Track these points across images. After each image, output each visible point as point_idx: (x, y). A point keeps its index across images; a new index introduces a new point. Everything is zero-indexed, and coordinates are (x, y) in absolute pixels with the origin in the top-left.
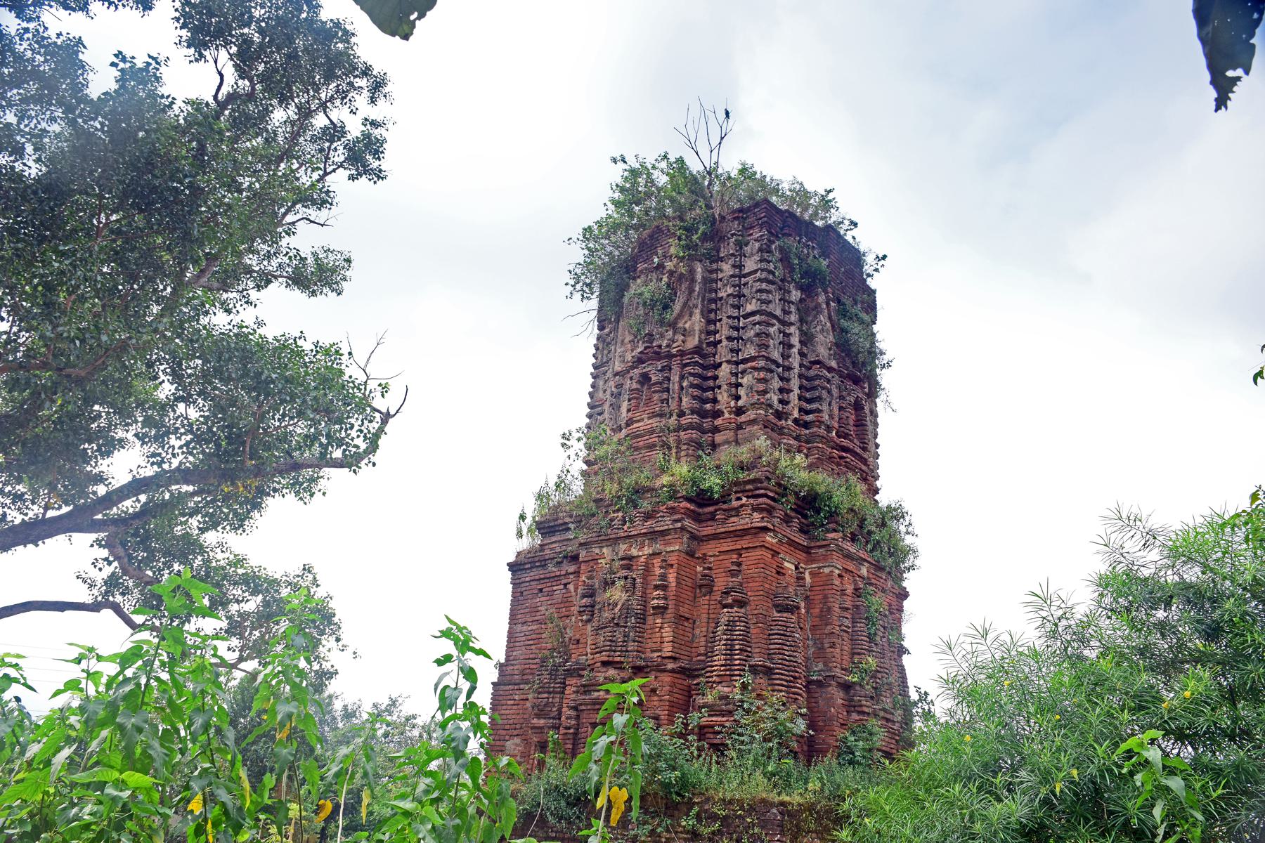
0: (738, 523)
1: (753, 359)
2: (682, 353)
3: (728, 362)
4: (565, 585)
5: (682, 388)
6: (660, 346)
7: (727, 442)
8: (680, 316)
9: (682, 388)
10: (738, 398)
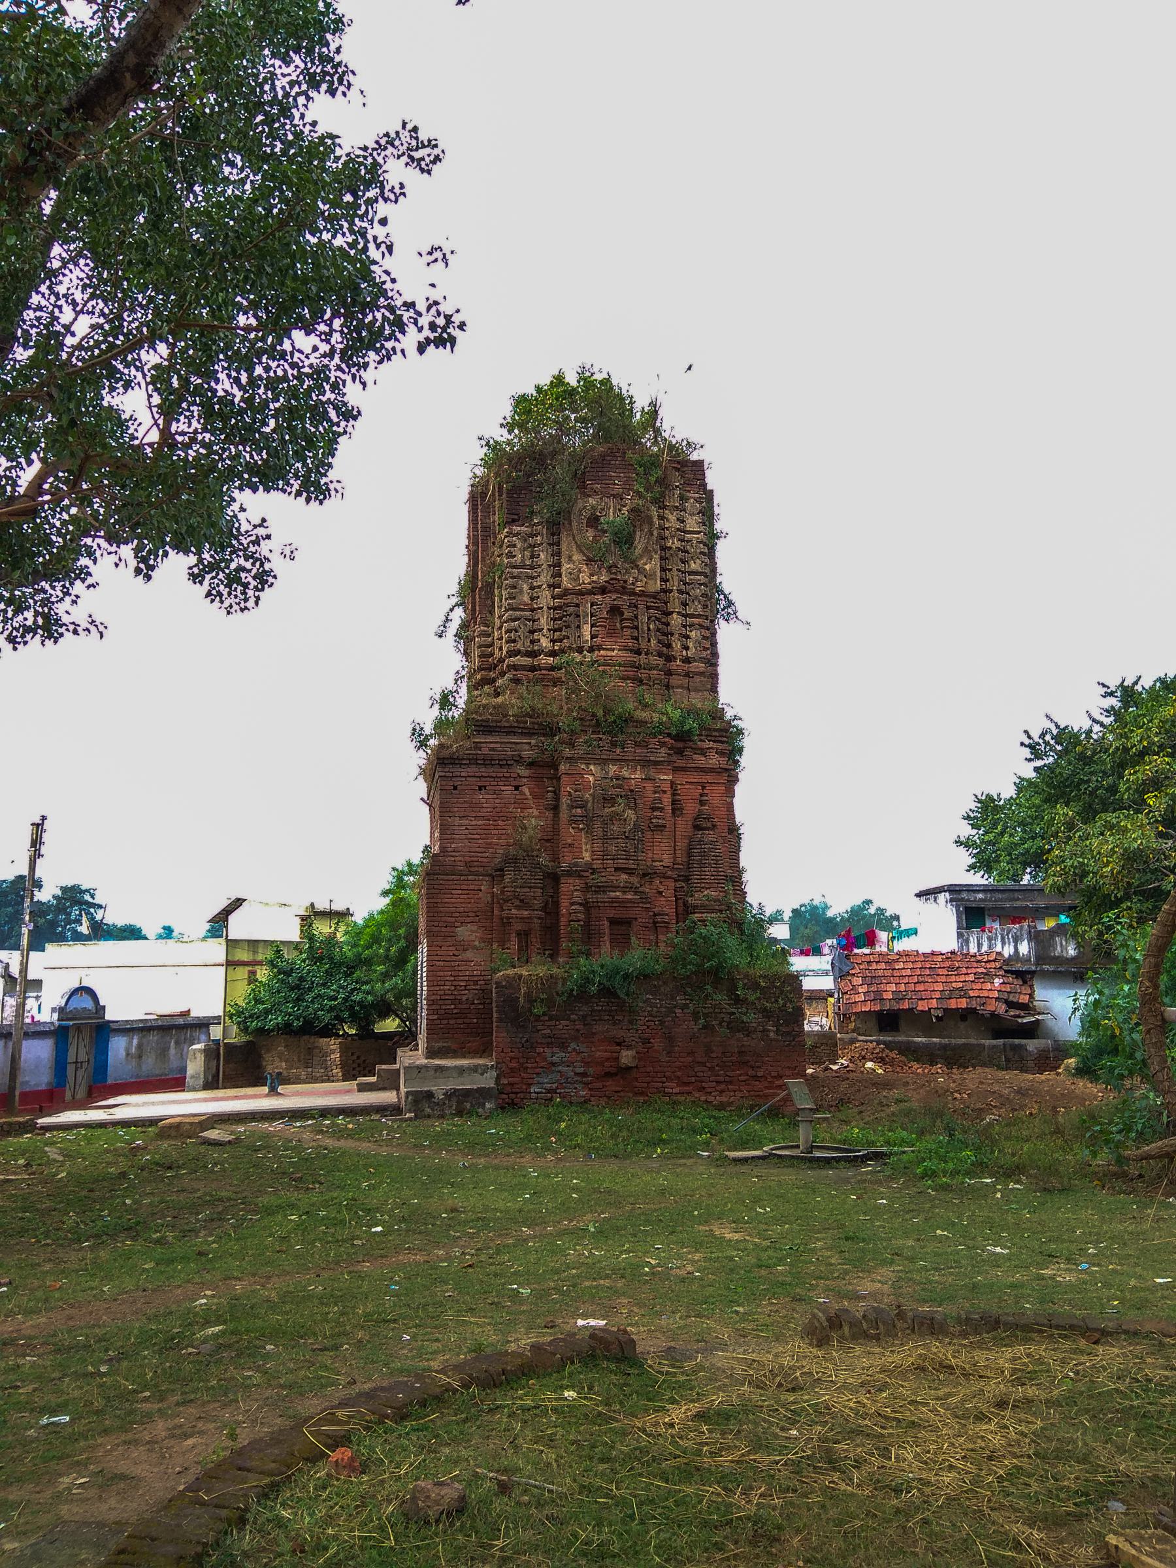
0: (700, 760)
1: (699, 616)
2: (643, 594)
3: (679, 613)
4: (517, 788)
5: (649, 629)
6: (625, 582)
7: (681, 687)
8: (641, 556)
9: (649, 629)
10: (687, 648)
